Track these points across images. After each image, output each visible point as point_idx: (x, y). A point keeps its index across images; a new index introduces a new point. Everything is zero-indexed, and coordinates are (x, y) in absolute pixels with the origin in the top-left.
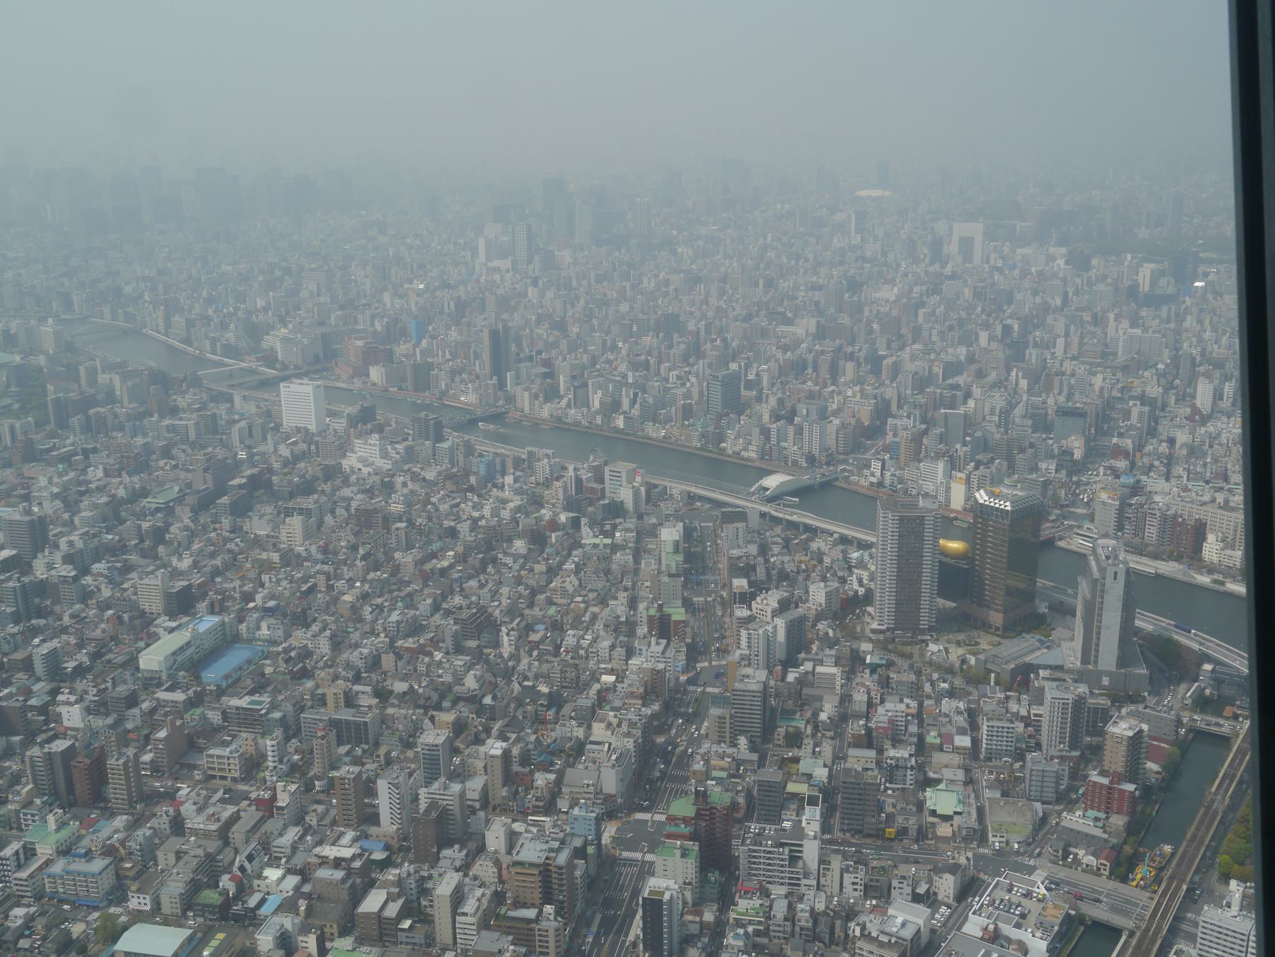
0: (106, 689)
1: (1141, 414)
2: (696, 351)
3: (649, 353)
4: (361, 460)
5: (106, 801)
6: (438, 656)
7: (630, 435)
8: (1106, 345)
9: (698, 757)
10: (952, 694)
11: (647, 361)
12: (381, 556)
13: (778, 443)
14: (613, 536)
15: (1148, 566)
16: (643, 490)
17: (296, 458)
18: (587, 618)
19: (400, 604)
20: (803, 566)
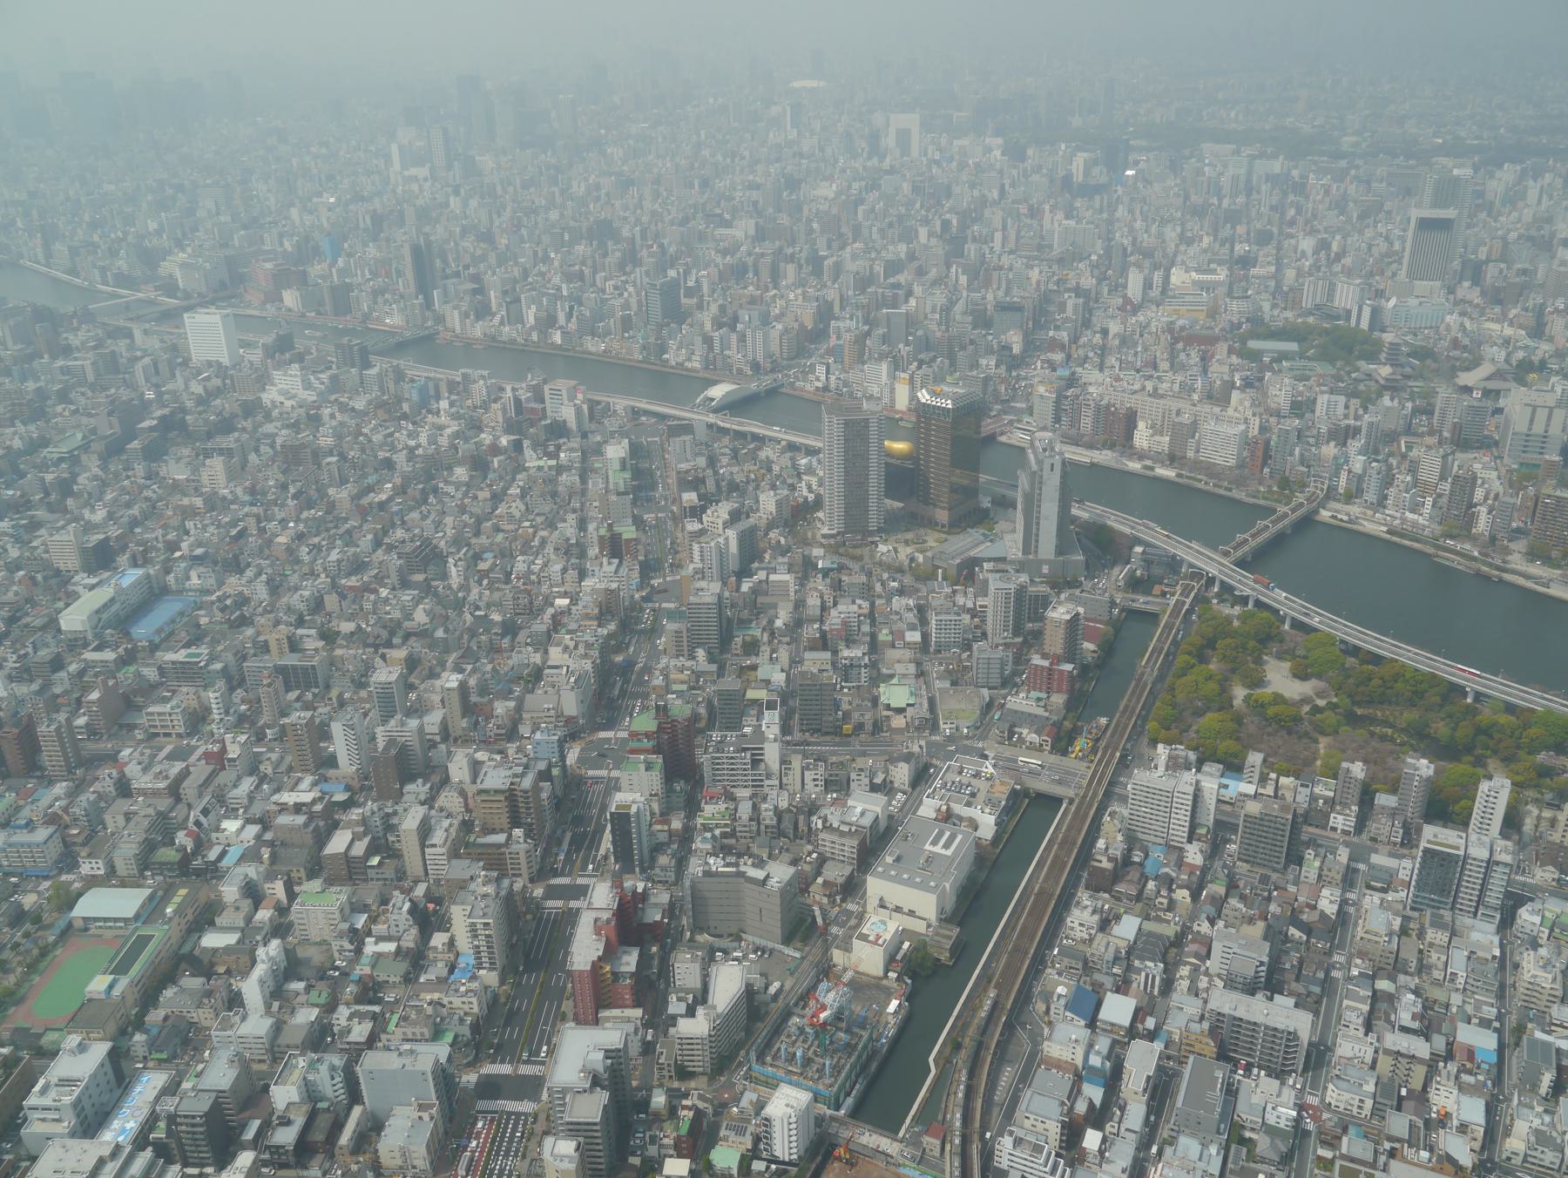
0: (26, 655)
1: (1076, 305)
2: (631, 259)
3: (583, 263)
4: (281, 392)
5: (42, 769)
6: (384, 592)
7: (568, 350)
8: (1042, 238)
9: (657, 673)
10: (901, 592)
11: (582, 272)
12: (314, 495)
14: (557, 457)
15: (1083, 456)
16: (585, 407)
17: (212, 394)
18: (536, 543)
19: (338, 542)
20: (753, 476)
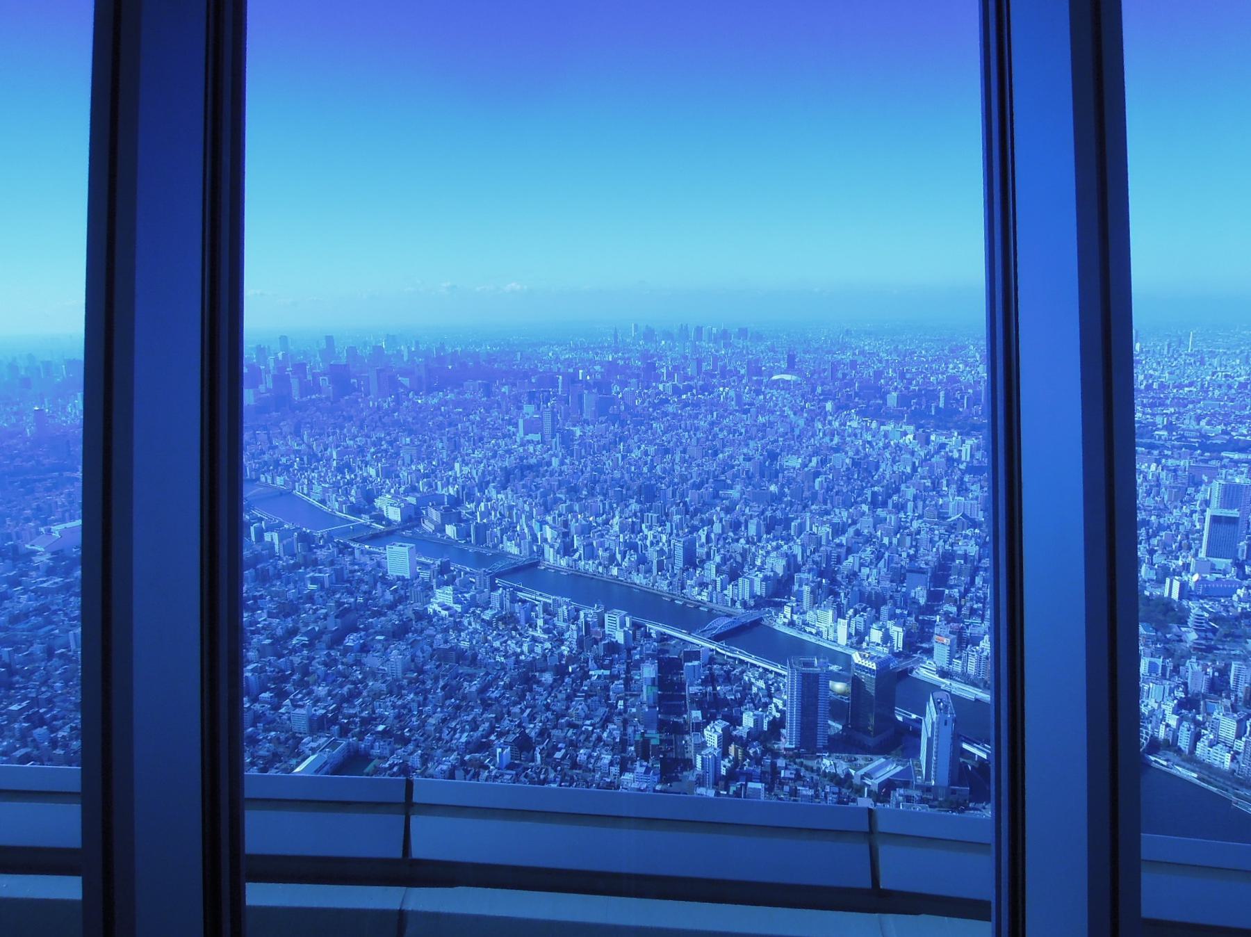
7: (622, 581)
13: (722, 591)
